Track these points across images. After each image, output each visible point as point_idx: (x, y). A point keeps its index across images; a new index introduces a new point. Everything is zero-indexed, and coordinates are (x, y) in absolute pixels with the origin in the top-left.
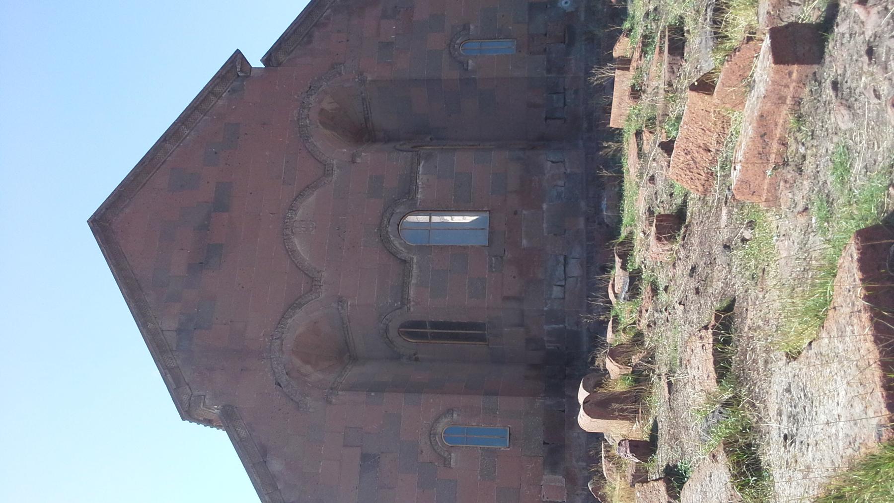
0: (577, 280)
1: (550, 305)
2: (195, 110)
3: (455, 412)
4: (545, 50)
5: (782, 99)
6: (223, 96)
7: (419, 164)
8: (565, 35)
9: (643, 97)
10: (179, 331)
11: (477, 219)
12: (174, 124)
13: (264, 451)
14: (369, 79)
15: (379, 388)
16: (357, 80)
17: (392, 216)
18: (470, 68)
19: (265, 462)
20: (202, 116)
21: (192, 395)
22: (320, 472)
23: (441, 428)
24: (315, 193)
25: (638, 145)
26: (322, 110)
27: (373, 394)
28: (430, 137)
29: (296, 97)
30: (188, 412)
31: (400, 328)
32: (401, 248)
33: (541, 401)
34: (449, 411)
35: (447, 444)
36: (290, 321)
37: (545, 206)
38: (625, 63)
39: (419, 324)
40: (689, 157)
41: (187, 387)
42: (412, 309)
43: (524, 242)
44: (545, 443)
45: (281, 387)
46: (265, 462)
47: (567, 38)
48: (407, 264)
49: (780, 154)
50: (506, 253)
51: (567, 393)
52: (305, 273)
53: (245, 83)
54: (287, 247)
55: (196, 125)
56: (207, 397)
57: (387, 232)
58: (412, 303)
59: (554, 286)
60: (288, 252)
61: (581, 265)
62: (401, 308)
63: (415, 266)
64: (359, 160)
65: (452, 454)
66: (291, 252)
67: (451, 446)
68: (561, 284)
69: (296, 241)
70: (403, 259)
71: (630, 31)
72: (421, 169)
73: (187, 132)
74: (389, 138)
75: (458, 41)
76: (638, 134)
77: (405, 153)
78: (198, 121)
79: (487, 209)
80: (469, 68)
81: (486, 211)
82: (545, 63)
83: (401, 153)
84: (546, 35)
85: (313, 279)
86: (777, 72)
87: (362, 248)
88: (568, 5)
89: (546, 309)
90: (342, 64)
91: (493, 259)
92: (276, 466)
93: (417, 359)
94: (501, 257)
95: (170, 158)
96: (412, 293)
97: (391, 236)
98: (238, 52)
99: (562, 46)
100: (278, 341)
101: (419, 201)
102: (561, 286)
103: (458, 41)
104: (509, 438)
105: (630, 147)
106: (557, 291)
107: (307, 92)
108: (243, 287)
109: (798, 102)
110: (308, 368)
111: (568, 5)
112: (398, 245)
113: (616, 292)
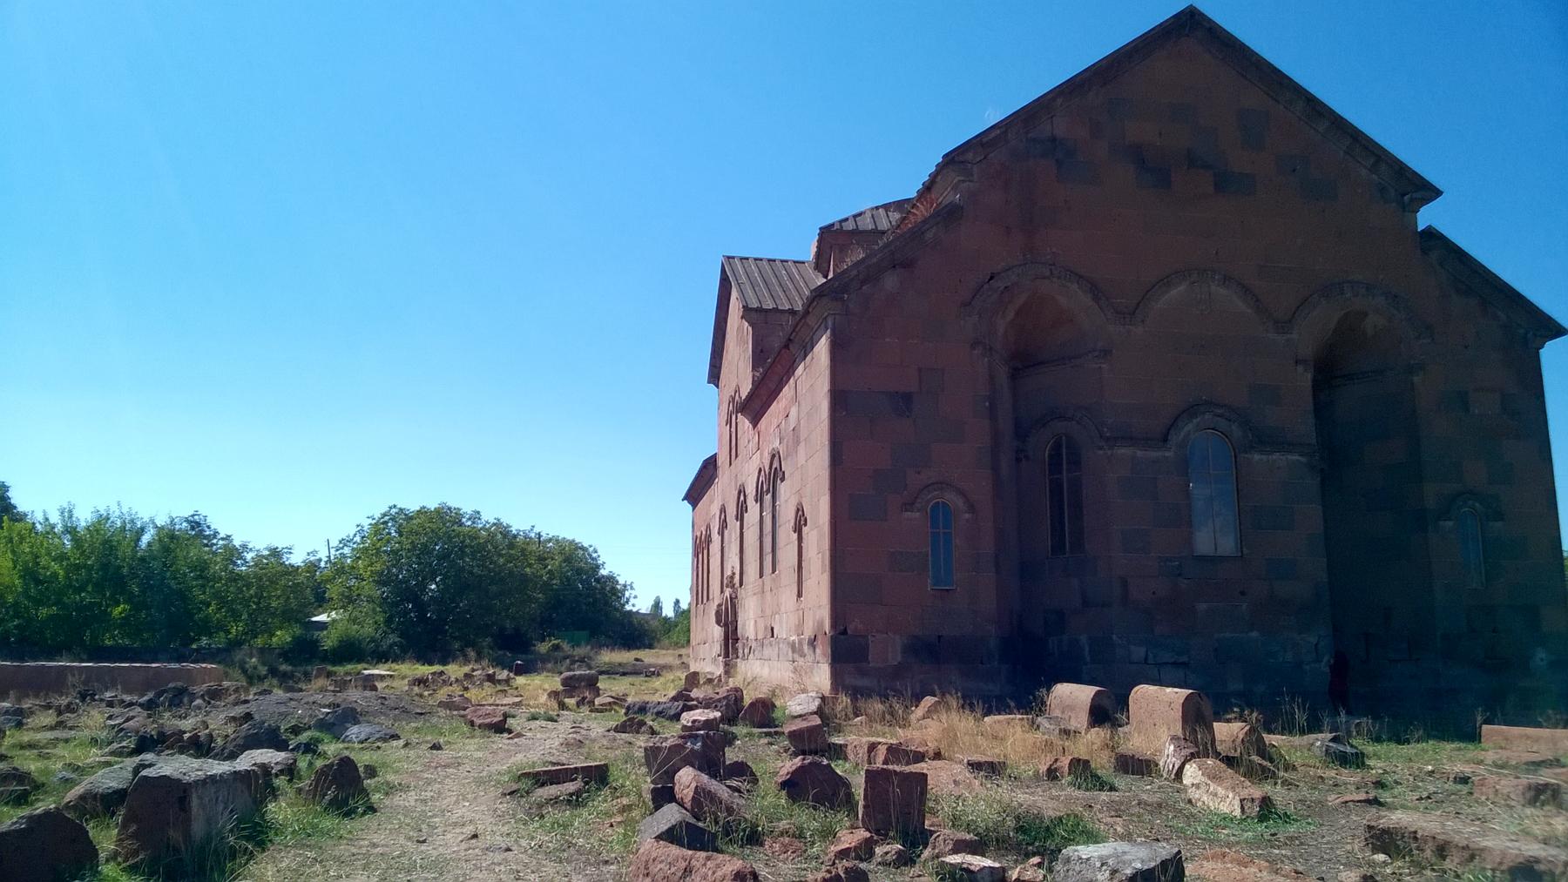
2: (1351, 136)
3: (971, 515)
7: (1300, 455)
10: (1053, 139)
12: (1332, 112)
13: (908, 265)
14: (1416, 379)
16: (1412, 362)
18: (1441, 523)
19: (894, 267)
24: (1249, 311)
26: (1366, 314)
27: (987, 404)
29: (1381, 277)
30: (953, 160)
32: (1182, 434)
33: (994, 630)
34: (972, 508)
36: (1075, 286)
37: (1254, 634)
39: (1076, 463)
41: (983, 157)
42: (1101, 452)
43: (1202, 607)
44: (939, 637)
46: (894, 267)
50: (1185, 581)
52: (1138, 304)
56: (971, 184)
57: (1204, 413)
58: (1109, 452)
59: (1145, 649)
60: (1168, 277)
62: (1101, 437)
64: (1300, 369)
66: (1168, 282)
69: (1182, 288)
72: (1296, 457)
74: (1321, 410)
79: (1244, 552)
81: (1242, 552)
84: (1494, 631)
89: (1114, 637)
91: (1177, 563)
92: (890, 281)
93: (1018, 460)
94: (1180, 575)
95: (1281, 107)
96: (1123, 451)
97: (1198, 419)
98: (1441, 193)
100: (1048, 274)
102: (1146, 659)
103: (1477, 505)
110: (1010, 315)
111: (1542, 663)
112: (1186, 429)
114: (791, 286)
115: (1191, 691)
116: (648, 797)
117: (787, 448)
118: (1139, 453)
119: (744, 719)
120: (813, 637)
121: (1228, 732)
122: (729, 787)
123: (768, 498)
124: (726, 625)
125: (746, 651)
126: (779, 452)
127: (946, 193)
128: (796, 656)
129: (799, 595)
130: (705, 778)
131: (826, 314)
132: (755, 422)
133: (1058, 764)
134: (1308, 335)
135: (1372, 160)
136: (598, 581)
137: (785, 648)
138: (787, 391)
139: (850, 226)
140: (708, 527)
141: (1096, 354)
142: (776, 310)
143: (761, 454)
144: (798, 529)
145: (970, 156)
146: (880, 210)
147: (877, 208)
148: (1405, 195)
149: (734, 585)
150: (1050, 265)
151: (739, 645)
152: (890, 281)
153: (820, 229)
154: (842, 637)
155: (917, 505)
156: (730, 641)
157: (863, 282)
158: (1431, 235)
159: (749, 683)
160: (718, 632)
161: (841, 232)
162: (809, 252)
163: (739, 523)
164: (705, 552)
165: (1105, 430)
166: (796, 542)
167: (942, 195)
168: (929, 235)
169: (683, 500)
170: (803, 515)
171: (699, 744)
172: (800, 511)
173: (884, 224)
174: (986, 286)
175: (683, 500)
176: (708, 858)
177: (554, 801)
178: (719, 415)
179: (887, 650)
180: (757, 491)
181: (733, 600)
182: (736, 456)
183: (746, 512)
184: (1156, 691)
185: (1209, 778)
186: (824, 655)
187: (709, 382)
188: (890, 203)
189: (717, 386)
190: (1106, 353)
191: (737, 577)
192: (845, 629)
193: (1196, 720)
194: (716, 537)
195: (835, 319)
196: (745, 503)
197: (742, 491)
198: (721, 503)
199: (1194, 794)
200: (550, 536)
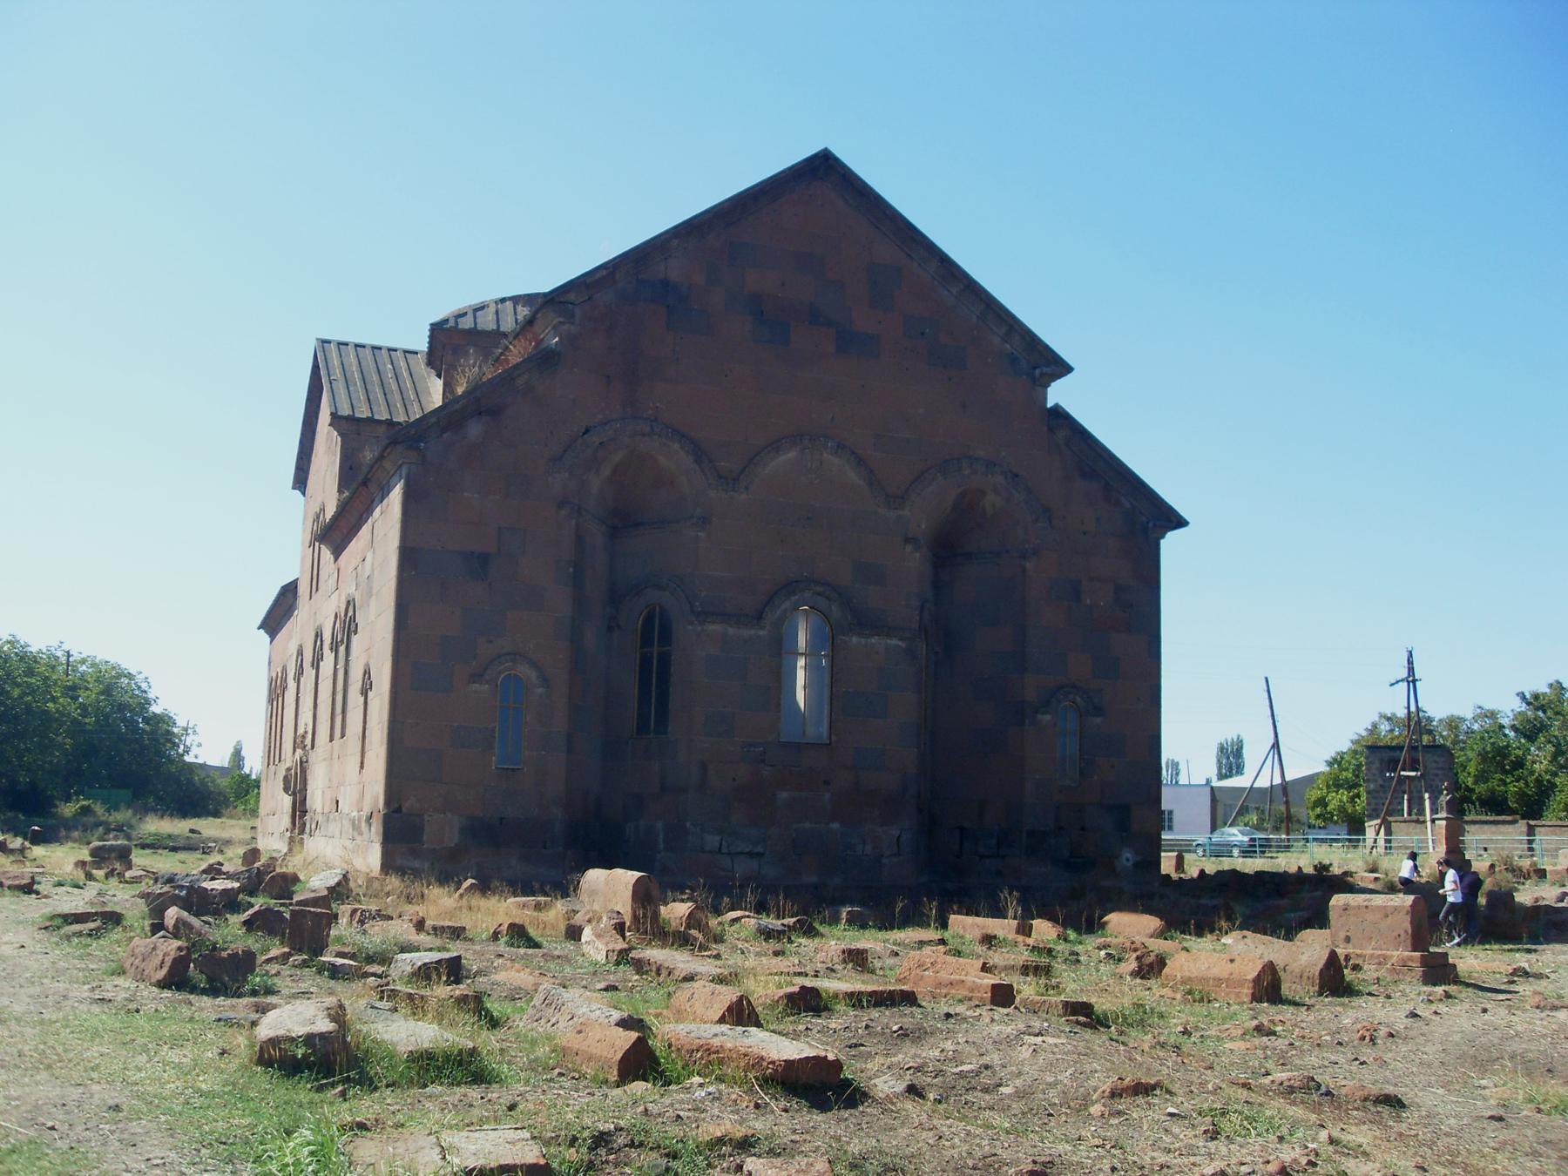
4: (1061, 828)
5: (972, 991)
7: (900, 640)
9: (984, 948)
10: (665, 283)
11: (799, 707)
13: (494, 412)
14: (1028, 565)
16: (1027, 546)
17: (827, 598)
18: (1039, 716)
19: (480, 414)
21: (574, 304)
22: (466, 494)
23: (526, 671)
25: (931, 941)
27: (571, 570)
31: (660, 607)
32: (778, 613)
34: (545, 681)
35: (502, 676)
36: (677, 446)
37: (835, 826)
38: (1025, 930)
39: (666, 636)
40: (929, 965)
41: (587, 298)
42: (690, 627)
43: (784, 795)
44: (501, 819)
45: (584, 434)
46: (480, 414)
48: (755, 621)
49: (940, 994)
50: (769, 768)
53: (1025, 377)
54: (784, 441)
56: (572, 327)
58: (699, 628)
62: (692, 611)
63: (753, 632)
64: (909, 548)
67: (497, 685)
68: (723, 847)
69: (792, 454)
70: (764, 616)
71: (1066, 940)
72: (894, 642)
73: (954, 292)
75: (1078, 699)
76: (942, 942)
77: (918, 618)
81: (830, 738)
83: (917, 612)
85: (736, 479)
86: (987, 986)
88: (1125, 862)
89: (688, 824)
90: (1050, 522)
91: (762, 749)
93: (610, 629)
94: (763, 761)
96: (715, 628)
97: (797, 597)
100: (647, 429)
101: (847, 639)
102: (720, 848)
103: (1078, 699)
104: (508, 769)
105: (931, 934)
106: (712, 841)
107: (1011, 471)
108: (726, 376)
109: (970, 999)
110: (606, 472)
111: (1125, 862)
113: (743, 920)
114: (394, 387)
115: (638, 874)
116: (148, 929)
117: (362, 595)
118: (731, 631)
119: (264, 890)
120: (369, 814)
121: (676, 911)
122: (203, 921)
123: (342, 649)
124: (294, 794)
125: (314, 826)
126: (354, 599)
127: (547, 331)
128: (355, 833)
129: (362, 767)
130: (185, 914)
131: (400, 462)
132: (337, 553)
133: (502, 927)
134: (921, 515)
135: (1004, 329)
136: (147, 721)
137: (347, 825)
138: (365, 530)
139: (466, 324)
140: (284, 670)
141: (695, 520)
142: (370, 420)
143: (340, 595)
144: (365, 692)
145: (572, 297)
146: (508, 303)
147: (503, 300)
148: (1035, 368)
149: (305, 746)
150: (652, 421)
151: (307, 817)
152: (474, 429)
153: (431, 325)
154: (396, 815)
155: (487, 677)
156: (298, 813)
157: (443, 430)
158: (1059, 414)
159: (310, 864)
160: (287, 800)
161: (455, 330)
162: (422, 344)
163: (314, 671)
164: (280, 699)
165: (697, 604)
166: (362, 707)
167: (544, 331)
168: (520, 381)
169: (259, 628)
170: (369, 678)
171: (184, 892)
172: (367, 673)
173: (508, 324)
175: (259, 628)
176: (165, 941)
177: (80, 934)
178: (304, 531)
179: (444, 830)
180: (333, 638)
181: (303, 765)
182: (317, 590)
183: (322, 660)
184: (622, 874)
185: (596, 937)
186: (377, 833)
187: (294, 488)
188: (520, 296)
189: (304, 494)
190: (704, 521)
191: (309, 736)
192: (400, 807)
193: (644, 897)
194: (291, 684)
195: (409, 469)
196: (322, 649)
197: (319, 635)
198: (298, 643)
199: (586, 949)
200: (84, 656)
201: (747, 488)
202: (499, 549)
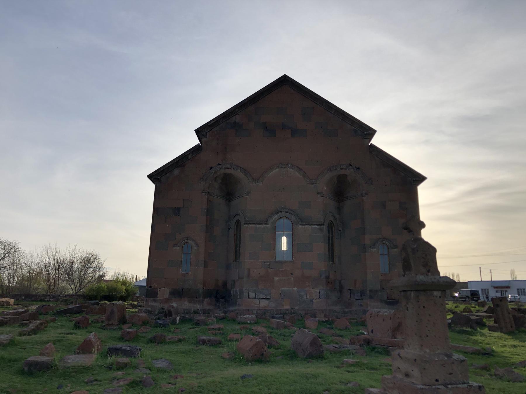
0: (258, 305)
1: (246, 291)
4: (383, 289)
6: (353, 127)
8: (392, 299)
10: (235, 123)
14: (364, 198)
15: (209, 212)
20: (341, 118)
24: (301, 176)
27: (206, 211)
28: (341, 230)
29: (353, 162)
30: (199, 132)
32: (274, 219)
37: (295, 289)
42: (245, 226)
43: (277, 279)
44: (183, 289)
47: (390, 300)
51: (206, 299)
55: (336, 116)
61: (265, 307)
63: (265, 226)
64: (319, 196)
65: (179, 248)
69: (277, 170)
75: (387, 243)
78: (339, 117)
80: (371, 249)
82: (375, 289)
87: (274, 201)
89: (244, 289)
99: (386, 298)
101: (298, 226)
103: (387, 243)
106: (252, 295)
108: (255, 148)
112: (275, 217)
118: (258, 226)
154: (149, 289)
155: (179, 245)
158: (373, 146)
174: (208, 172)
201: (262, 181)
202: (183, 206)
